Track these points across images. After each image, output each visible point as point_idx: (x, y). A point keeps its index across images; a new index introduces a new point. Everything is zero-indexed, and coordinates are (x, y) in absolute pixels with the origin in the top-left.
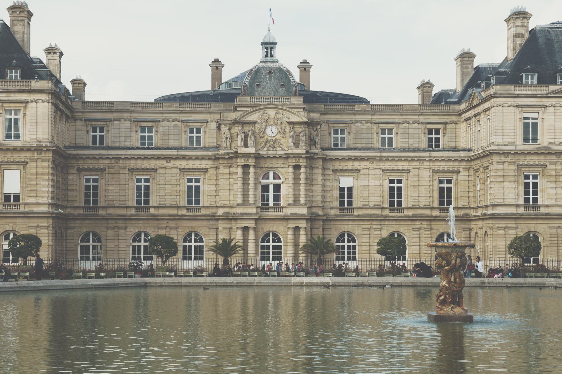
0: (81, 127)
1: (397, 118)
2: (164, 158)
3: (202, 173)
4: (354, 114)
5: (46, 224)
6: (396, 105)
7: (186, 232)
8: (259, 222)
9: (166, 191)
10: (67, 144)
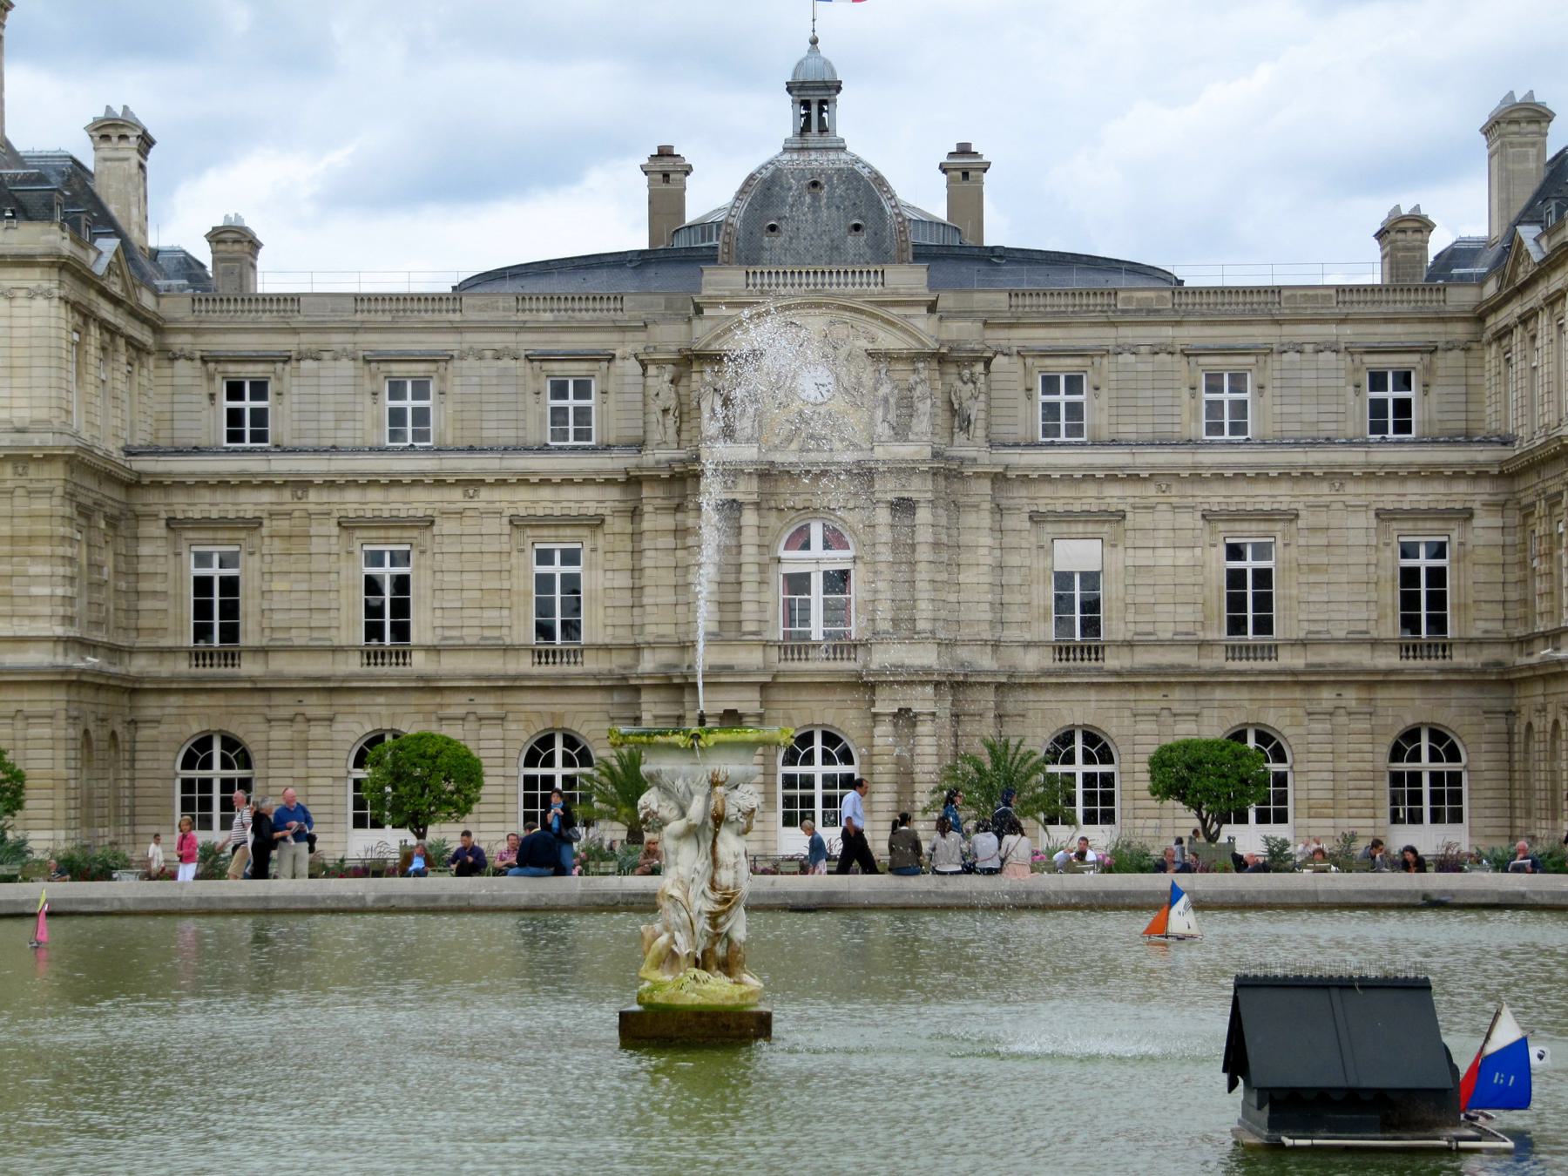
0: (189, 381)
1: (1260, 334)
2: (458, 483)
3: (585, 532)
4: (1113, 324)
5: (45, 708)
6: (1259, 290)
7: (533, 732)
8: (776, 695)
9: (466, 594)
10: (140, 439)
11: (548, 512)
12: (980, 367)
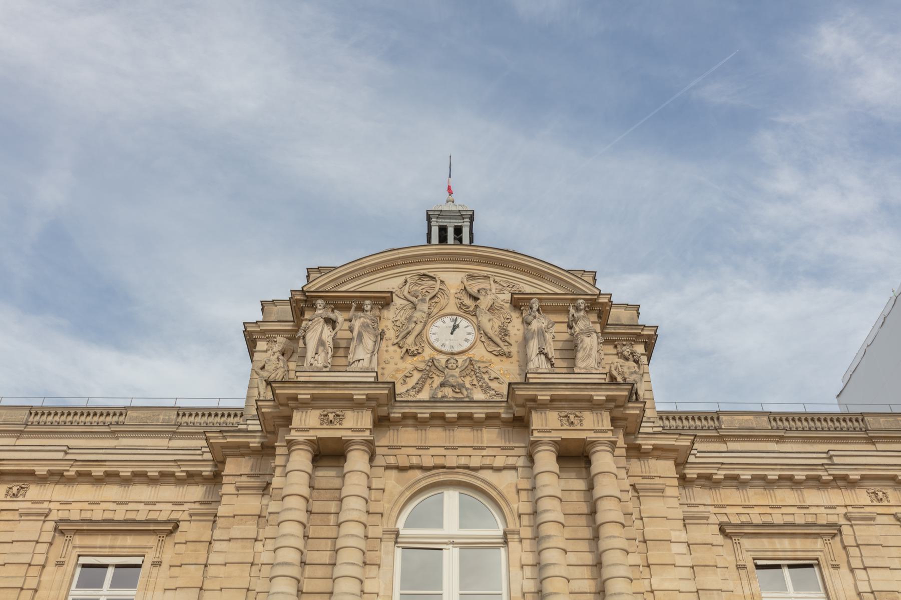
3: (151, 540)
11: (108, 515)
12: (640, 349)
